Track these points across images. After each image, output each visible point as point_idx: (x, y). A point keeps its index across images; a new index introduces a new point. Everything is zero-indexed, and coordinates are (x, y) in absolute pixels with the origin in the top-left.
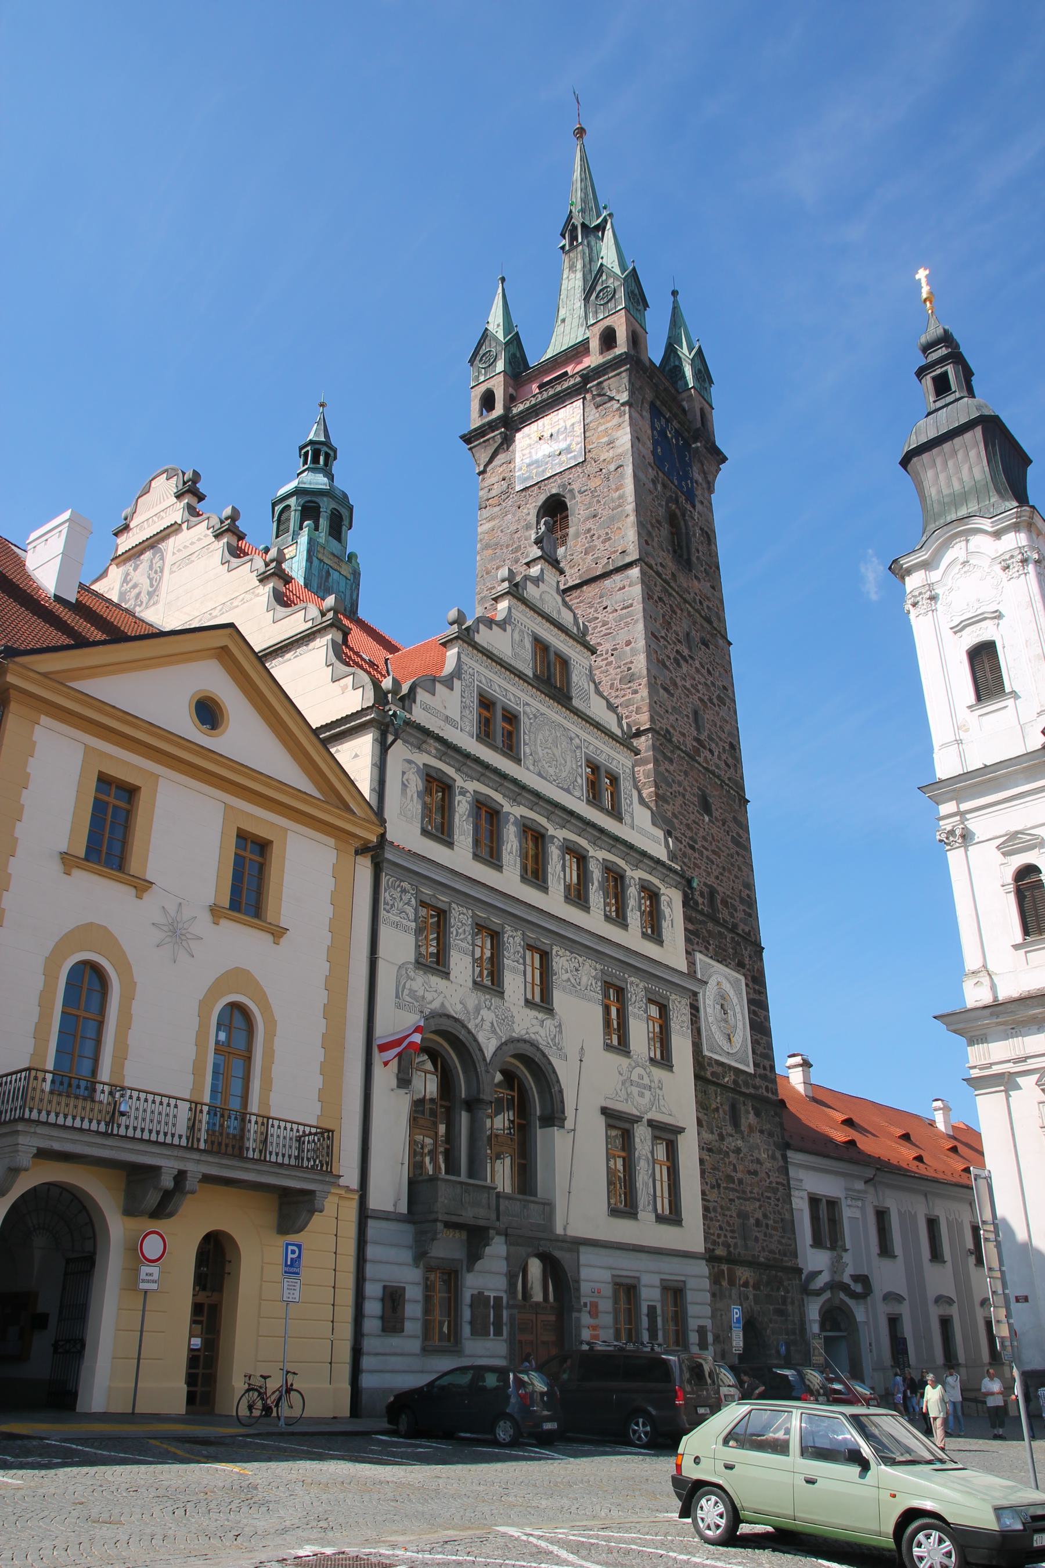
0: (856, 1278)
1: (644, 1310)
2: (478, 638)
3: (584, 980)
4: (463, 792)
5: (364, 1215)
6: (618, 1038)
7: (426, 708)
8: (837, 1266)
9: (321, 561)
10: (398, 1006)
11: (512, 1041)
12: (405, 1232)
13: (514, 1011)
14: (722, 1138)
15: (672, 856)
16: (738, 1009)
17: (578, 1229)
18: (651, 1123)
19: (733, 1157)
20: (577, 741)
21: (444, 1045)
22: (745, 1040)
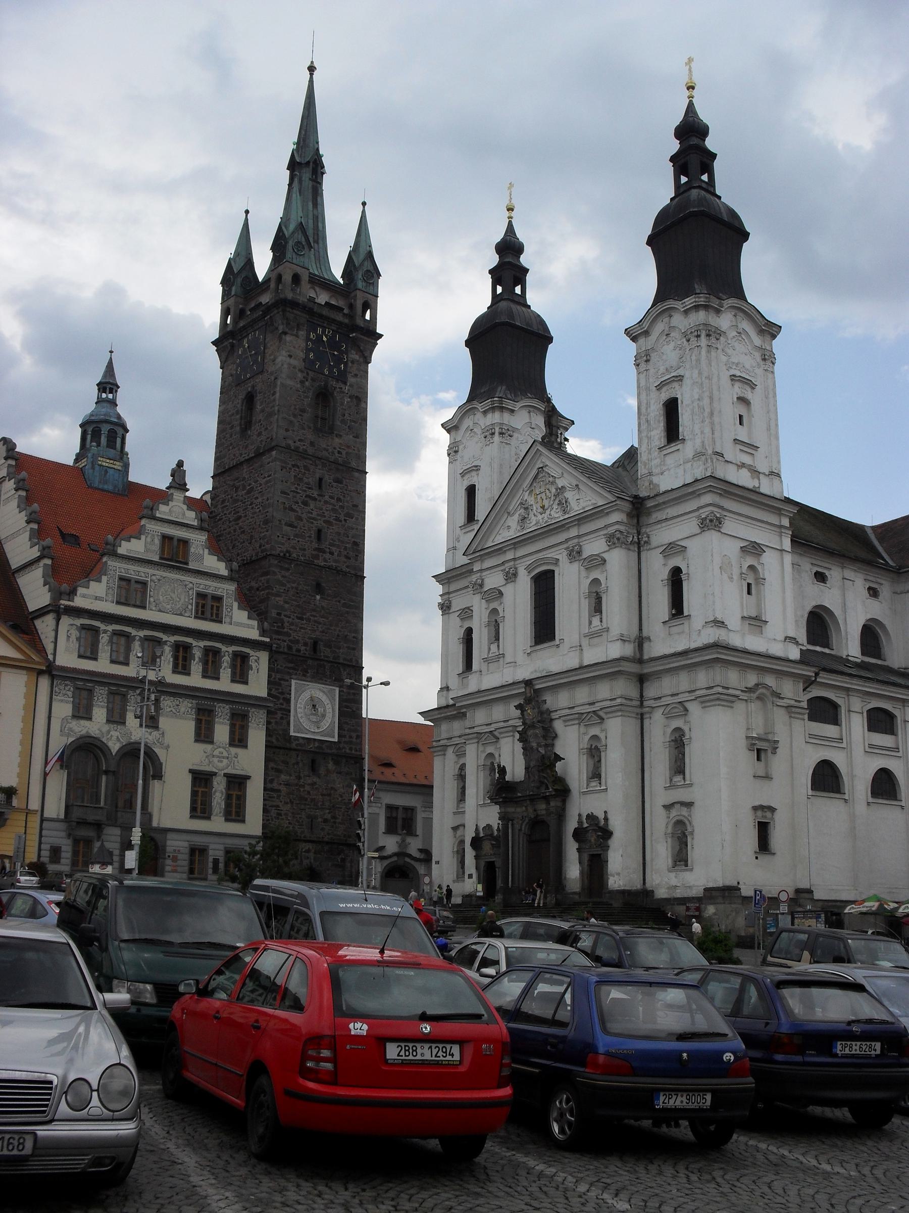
0: (421, 850)
1: (211, 859)
2: (121, 551)
3: (183, 710)
4: (105, 632)
5: (43, 820)
6: (204, 734)
7: (84, 596)
8: (402, 844)
9: (101, 465)
10: (61, 735)
11: (130, 744)
12: (62, 826)
13: (132, 730)
14: (299, 778)
15: (263, 633)
16: (329, 707)
17: (167, 823)
18: (225, 775)
19: (307, 788)
20: (191, 585)
21: (85, 750)
22: (333, 722)
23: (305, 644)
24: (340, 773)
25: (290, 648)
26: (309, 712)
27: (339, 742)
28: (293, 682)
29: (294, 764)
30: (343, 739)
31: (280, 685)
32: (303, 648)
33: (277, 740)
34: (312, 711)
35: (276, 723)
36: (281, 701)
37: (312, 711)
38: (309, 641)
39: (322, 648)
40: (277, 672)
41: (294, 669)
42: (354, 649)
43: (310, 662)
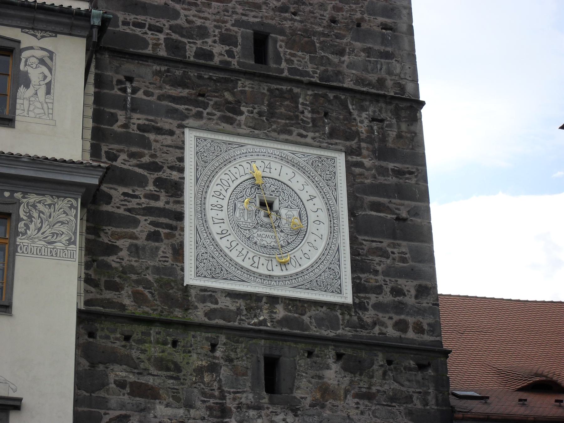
22: (331, 248)
23: (227, 39)
24: (368, 396)
25: (174, 47)
26: (247, 220)
27: (359, 305)
28: (190, 138)
29: (200, 371)
30: (373, 298)
31: (147, 144)
32: (218, 49)
33: (138, 297)
34: (255, 216)
35: (135, 250)
36: (151, 187)
37: (255, 216)
38: (238, 32)
39: (282, 49)
40: (134, 110)
41: (196, 104)
42: (387, 55)
43: (245, 85)
